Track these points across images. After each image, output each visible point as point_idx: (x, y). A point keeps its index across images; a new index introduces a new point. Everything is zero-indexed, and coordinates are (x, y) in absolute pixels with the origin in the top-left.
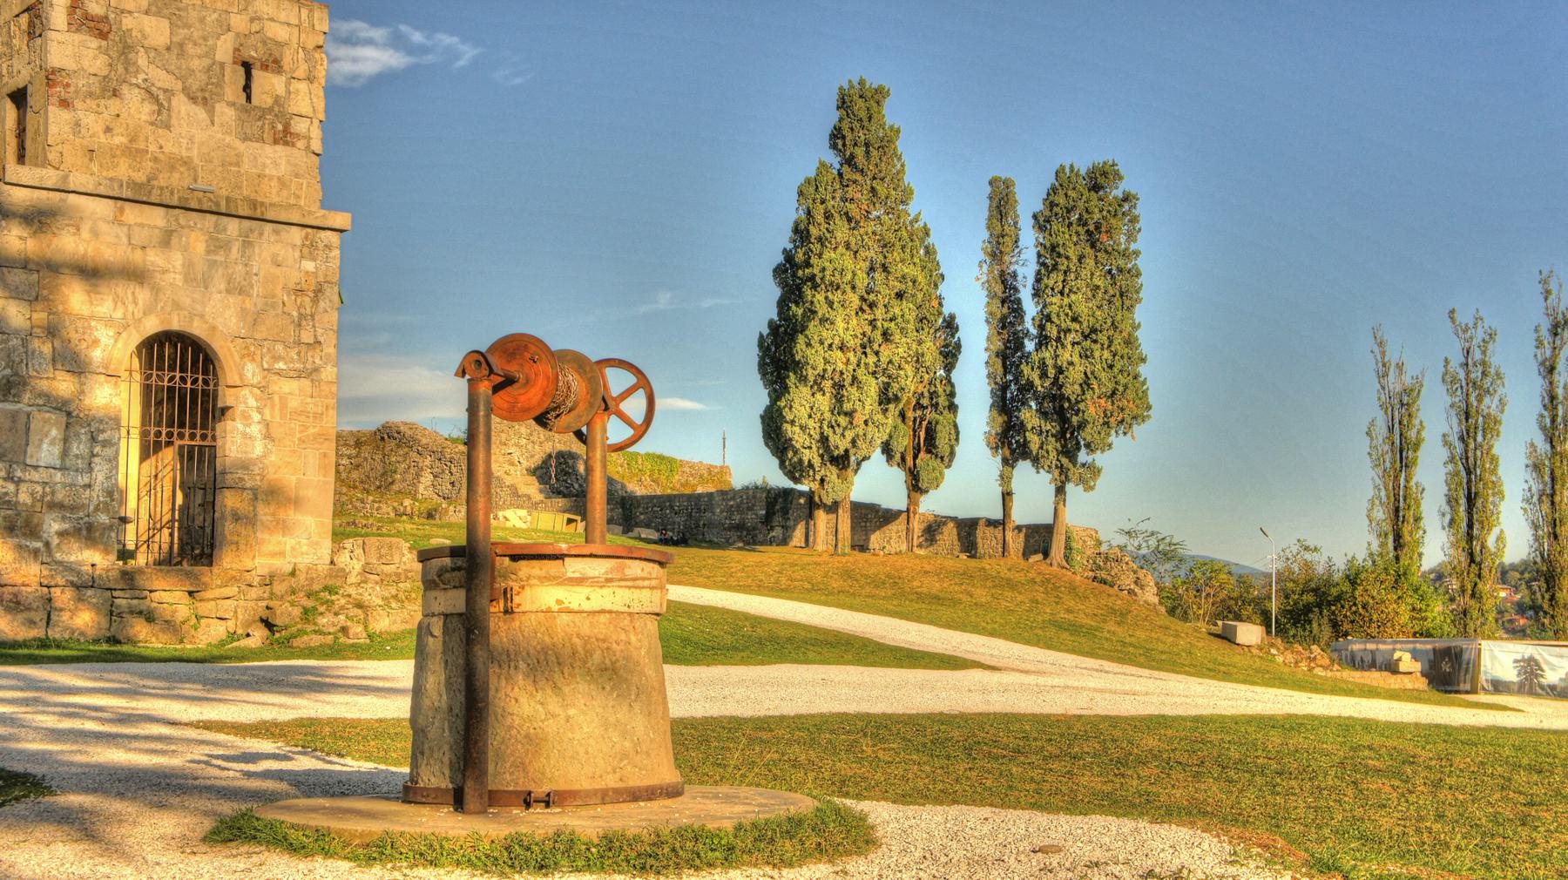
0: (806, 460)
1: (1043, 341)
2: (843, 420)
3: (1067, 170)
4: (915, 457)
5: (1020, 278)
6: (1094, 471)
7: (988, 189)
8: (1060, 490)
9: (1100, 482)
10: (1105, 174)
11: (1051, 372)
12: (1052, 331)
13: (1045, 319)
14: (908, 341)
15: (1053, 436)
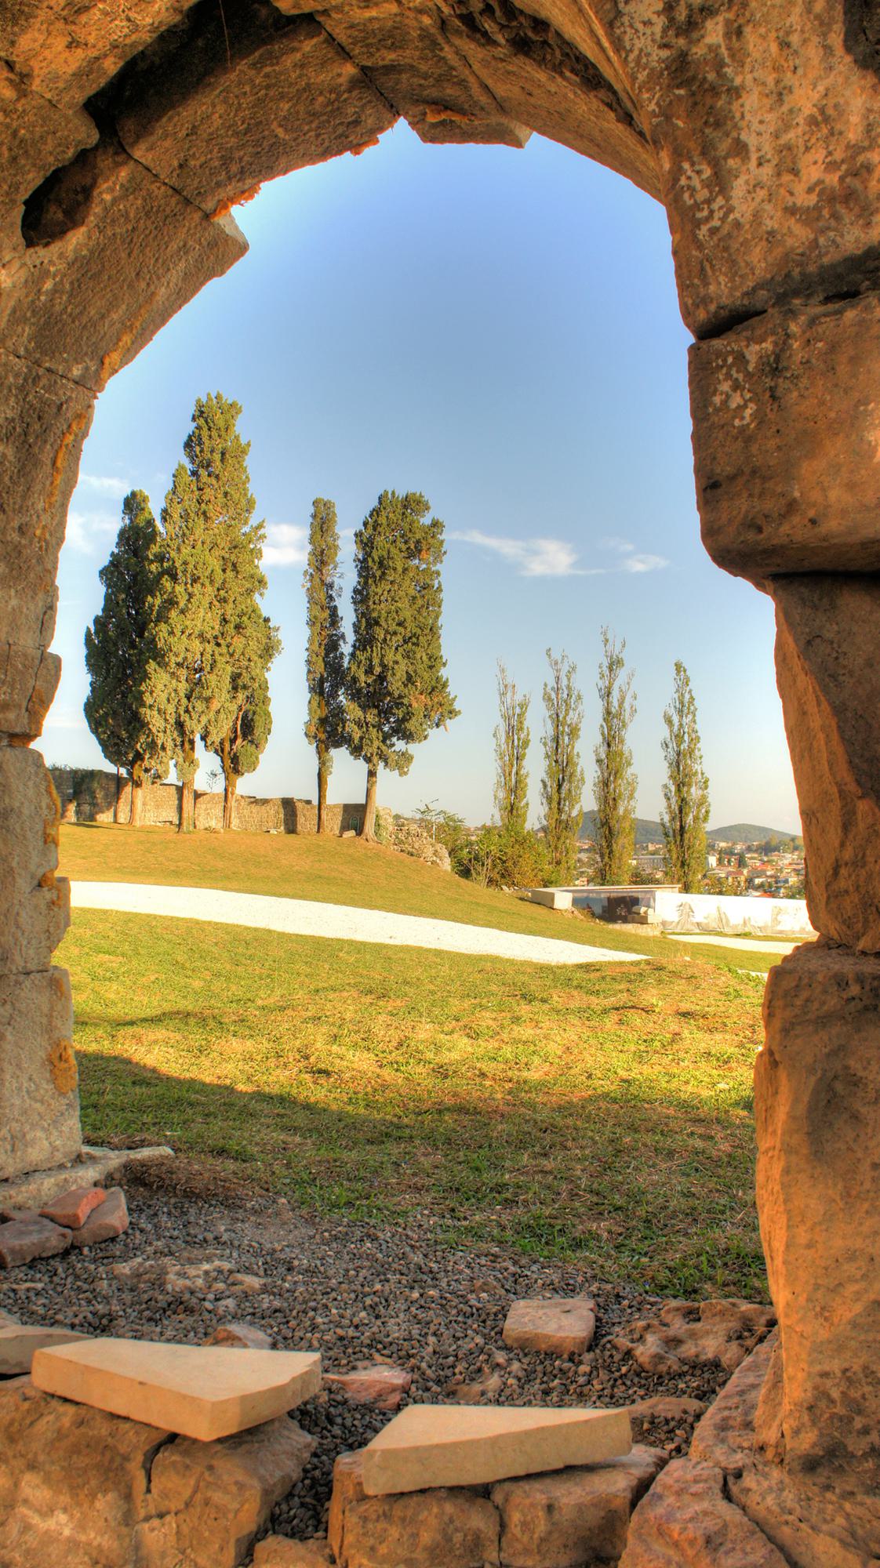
0: (159, 742)
1: (364, 642)
2: (200, 706)
3: (390, 496)
4: (233, 741)
5: (336, 587)
6: (406, 758)
7: (312, 510)
8: (372, 774)
9: (413, 767)
10: (419, 503)
11: (378, 670)
12: (380, 633)
13: (367, 625)
14: (259, 635)
15: (374, 727)
